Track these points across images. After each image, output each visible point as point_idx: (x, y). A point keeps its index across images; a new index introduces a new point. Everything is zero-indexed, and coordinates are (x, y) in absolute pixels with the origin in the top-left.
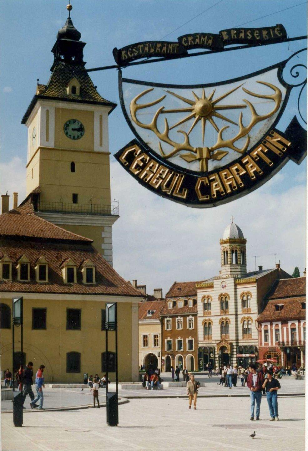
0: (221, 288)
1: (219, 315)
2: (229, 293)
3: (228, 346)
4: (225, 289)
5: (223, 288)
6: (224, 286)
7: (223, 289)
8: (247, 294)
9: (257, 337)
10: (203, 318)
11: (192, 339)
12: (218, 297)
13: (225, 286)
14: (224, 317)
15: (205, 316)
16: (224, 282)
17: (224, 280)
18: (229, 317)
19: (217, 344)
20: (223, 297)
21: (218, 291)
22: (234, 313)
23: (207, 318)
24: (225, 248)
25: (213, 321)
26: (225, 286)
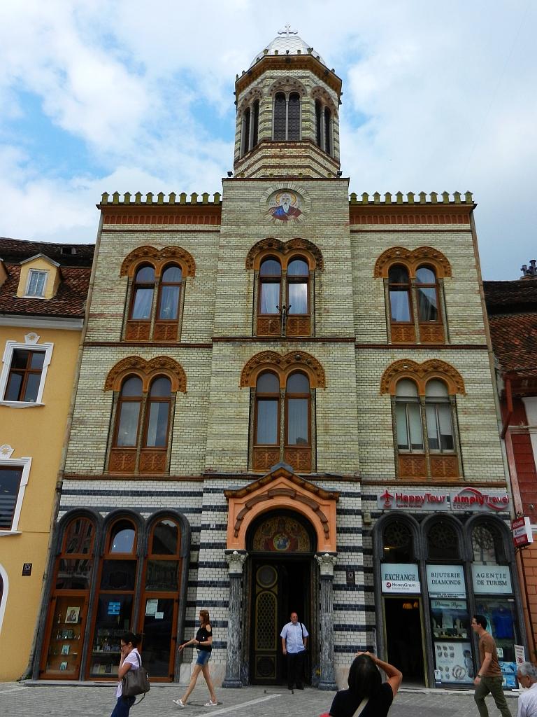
0: (270, 217)
1: (243, 340)
5: (284, 217)
6: (286, 209)
7: (278, 221)
10: (112, 357)
11: (15, 461)
12: (243, 254)
13: (291, 209)
15: (134, 345)
16: (289, 196)
17: (291, 185)
18: (314, 350)
19: (232, 495)
21: (253, 229)
23: (148, 355)
25: (189, 372)
26: (291, 209)
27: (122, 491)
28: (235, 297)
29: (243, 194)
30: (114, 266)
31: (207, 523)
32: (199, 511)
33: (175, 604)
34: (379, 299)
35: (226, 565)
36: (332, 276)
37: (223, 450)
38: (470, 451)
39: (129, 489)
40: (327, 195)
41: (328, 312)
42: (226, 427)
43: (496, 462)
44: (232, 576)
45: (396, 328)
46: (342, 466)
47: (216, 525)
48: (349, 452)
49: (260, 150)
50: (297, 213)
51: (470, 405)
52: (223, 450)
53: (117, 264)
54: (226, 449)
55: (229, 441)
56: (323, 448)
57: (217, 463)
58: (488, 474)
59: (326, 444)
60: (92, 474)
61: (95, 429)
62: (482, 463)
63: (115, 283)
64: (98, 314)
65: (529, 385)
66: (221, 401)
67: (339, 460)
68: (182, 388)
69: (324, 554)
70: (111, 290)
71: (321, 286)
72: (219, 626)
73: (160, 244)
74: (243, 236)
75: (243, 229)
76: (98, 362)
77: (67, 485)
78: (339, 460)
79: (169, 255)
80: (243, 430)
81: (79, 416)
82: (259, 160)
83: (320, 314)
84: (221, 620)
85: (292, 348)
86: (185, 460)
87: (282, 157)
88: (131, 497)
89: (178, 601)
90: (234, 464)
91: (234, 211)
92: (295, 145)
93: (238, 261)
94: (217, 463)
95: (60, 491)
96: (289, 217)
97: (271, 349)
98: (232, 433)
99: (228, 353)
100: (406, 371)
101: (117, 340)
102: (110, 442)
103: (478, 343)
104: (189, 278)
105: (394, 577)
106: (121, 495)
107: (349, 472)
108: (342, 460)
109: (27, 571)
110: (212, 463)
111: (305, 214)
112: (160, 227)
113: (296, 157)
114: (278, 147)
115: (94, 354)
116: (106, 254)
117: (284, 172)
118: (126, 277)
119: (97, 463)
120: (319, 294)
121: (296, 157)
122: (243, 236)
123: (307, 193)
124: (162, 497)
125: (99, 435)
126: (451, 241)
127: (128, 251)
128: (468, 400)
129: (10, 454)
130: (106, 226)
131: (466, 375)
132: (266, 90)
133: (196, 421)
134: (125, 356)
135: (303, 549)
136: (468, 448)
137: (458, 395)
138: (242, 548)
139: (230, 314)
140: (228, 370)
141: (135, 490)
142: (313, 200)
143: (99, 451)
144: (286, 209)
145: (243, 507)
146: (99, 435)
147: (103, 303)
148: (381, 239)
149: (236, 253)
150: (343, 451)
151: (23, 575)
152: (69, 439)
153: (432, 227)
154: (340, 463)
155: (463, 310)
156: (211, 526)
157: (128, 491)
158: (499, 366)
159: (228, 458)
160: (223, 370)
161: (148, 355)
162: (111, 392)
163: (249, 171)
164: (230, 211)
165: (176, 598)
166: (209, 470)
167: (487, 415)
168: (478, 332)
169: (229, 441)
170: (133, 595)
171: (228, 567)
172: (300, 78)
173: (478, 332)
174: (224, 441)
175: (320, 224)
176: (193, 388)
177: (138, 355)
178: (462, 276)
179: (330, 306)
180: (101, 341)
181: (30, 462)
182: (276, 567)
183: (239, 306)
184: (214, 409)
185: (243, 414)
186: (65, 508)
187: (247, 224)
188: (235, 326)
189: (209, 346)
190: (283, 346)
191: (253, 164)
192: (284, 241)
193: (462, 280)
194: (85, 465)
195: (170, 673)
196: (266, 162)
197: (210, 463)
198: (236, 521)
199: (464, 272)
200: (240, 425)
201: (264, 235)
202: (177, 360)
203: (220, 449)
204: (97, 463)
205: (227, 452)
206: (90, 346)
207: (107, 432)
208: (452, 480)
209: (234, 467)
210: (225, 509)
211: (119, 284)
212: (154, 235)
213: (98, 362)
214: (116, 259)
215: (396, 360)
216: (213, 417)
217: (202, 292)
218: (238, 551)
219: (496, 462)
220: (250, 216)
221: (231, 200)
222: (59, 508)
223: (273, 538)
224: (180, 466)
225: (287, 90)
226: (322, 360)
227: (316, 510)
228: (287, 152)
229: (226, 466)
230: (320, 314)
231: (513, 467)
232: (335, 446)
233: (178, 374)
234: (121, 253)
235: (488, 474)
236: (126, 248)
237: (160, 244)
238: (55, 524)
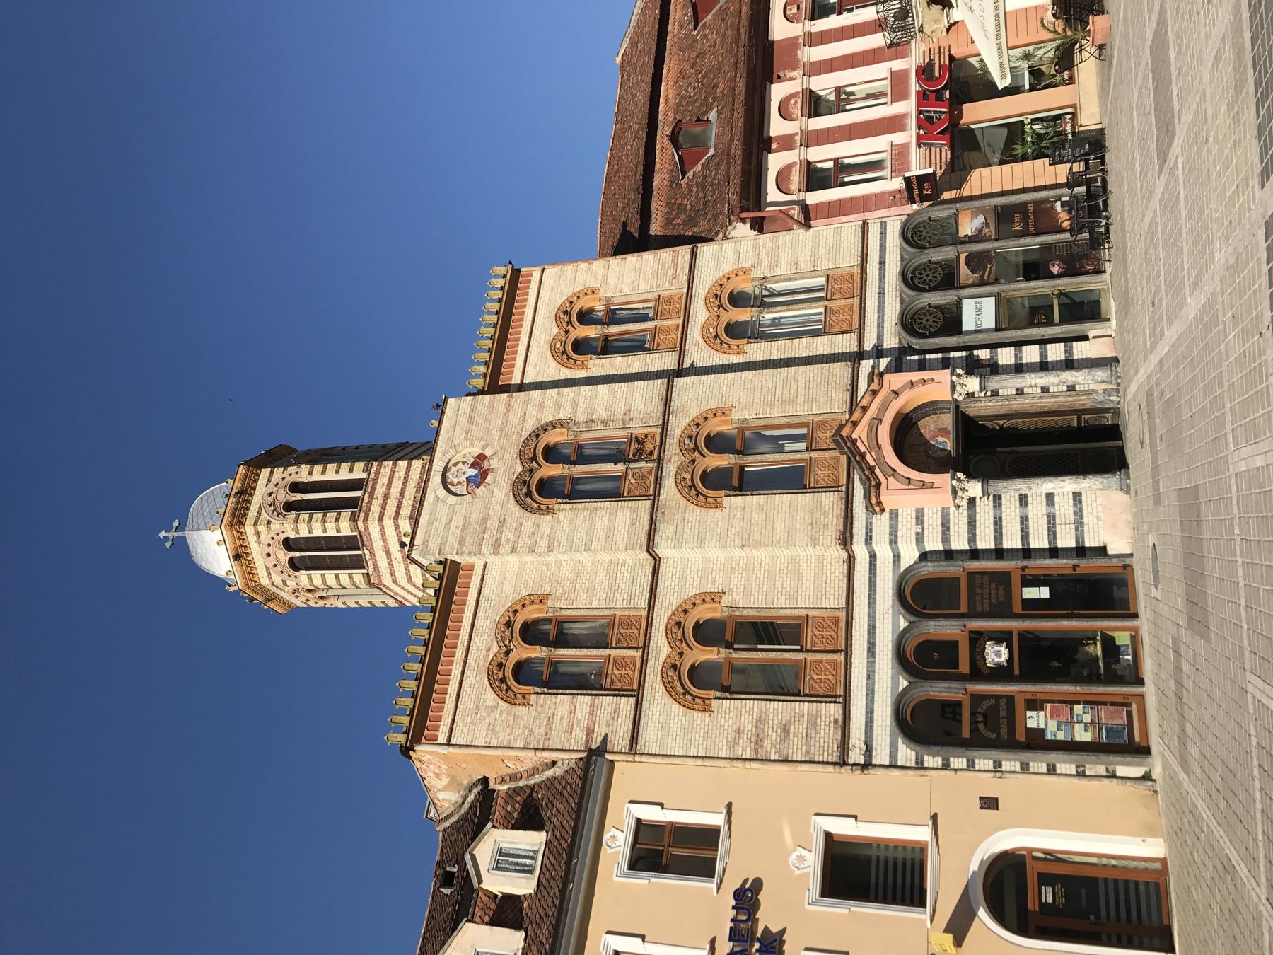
2: (529, 427)
3: (896, 393)
4: (493, 463)
5: (484, 474)
6: (474, 472)
7: (489, 480)
8: (569, 322)
9: (848, 227)
11: (818, 845)
12: (530, 519)
14: (673, 461)
20: (537, 477)
21: (495, 514)
22: (660, 384)
23: (661, 648)
24: (270, 500)
25: (692, 590)
26: (473, 466)
27: (868, 671)
28: (591, 526)
29: (437, 528)
30: (511, 718)
31: (914, 536)
32: (897, 557)
33: (1027, 572)
34: (617, 363)
35: (972, 501)
36: (580, 410)
37: (812, 524)
38: (823, 260)
39: (865, 661)
40: (463, 422)
41: (630, 411)
42: (779, 523)
43: (837, 233)
44: (985, 493)
45: (662, 314)
46: (838, 382)
47: (917, 524)
48: (820, 374)
49: (366, 529)
50: (482, 457)
51: (766, 262)
52: (812, 524)
53: (509, 714)
54: (810, 521)
55: (798, 518)
56: (814, 405)
57: (830, 530)
58: (853, 242)
59: (809, 401)
60: (840, 720)
61: (771, 722)
62: (838, 247)
63: (540, 714)
64: (588, 735)
65: (748, 200)
66: (740, 531)
67: (830, 386)
68: (714, 598)
69: (952, 382)
70: (551, 718)
71: (592, 421)
72: (1053, 511)
73: (489, 650)
74: (502, 523)
75: (493, 524)
76: (664, 728)
77: (856, 756)
78: (830, 386)
79: (508, 633)
80: (784, 502)
81: (748, 749)
82: (382, 528)
83: (631, 420)
84: (1044, 509)
85: (672, 449)
86: (824, 585)
87: (386, 496)
88: (877, 656)
89: (1023, 568)
90: (831, 509)
91: (461, 537)
92: (374, 480)
93: (538, 526)
94: (830, 530)
95: (867, 766)
96: (486, 468)
97: (672, 474)
98: (787, 516)
99: (672, 528)
100: (716, 329)
101: (632, 700)
102: (793, 698)
103: (687, 257)
104: (550, 603)
105: (979, 322)
106: (874, 672)
107: (846, 374)
108: (830, 382)
109: (990, 803)
110: (829, 537)
111: (483, 448)
112: (460, 653)
113: (391, 478)
114: (370, 503)
115: (650, 737)
116: (490, 732)
117: (411, 491)
118: (533, 697)
119: (823, 713)
120: (602, 422)
121: (391, 478)
122: (502, 523)
123: (455, 447)
124: (877, 612)
125: (780, 714)
126: (553, 289)
127: (490, 696)
128: (760, 264)
129: (804, 852)
130: (442, 738)
131: (728, 267)
132: (275, 526)
133: (766, 575)
134: (660, 688)
135: (947, 420)
136: (819, 262)
137: (753, 274)
138: (948, 476)
139: (616, 530)
140: (697, 526)
141: (865, 653)
142: (466, 438)
143: (806, 712)
144: (474, 472)
145: (891, 479)
146: (780, 714)
147: (570, 729)
148: (536, 365)
149: (526, 530)
150: (819, 381)
151: (997, 809)
152: (786, 761)
153: (529, 311)
154: (834, 384)
155: (645, 273)
156: (919, 530)
157: (868, 662)
158: (721, 235)
159: (822, 517)
160: (696, 532)
161: (661, 648)
162: (715, 703)
163: (392, 550)
164: (460, 543)
165: (1020, 572)
166: (839, 539)
167: (781, 245)
168: (675, 260)
169: (798, 518)
170: (1020, 634)
171: (974, 499)
172: (269, 481)
173: (675, 260)
174: (798, 524)
175: (504, 425)
176: (717, 584)
177: (660, 667)
178: (600, 277)
179: (621, 408)
180: (631, 726)
181: (820, 819)
182: (971, 457)
183: (606, 519)
184: (751, 541)
185: (761, 503)
186: (893, 754)
187: (485, 520)
188: (633, 523)
189: (657, 561)
190: (670, 460)
191: (384, 541)
192: (519, 468)
193: (606, 276)
194: (827, 731)
195: (1121, 571)
196: (390, 516)
197: (829, 540)
198: (911, 487)
199: (596, 274)
200: (776, 506)
201: (507, 495)
202: (674, 608)
203: (810, 528)
204: (823, 713)
205: (814, 519)
206: (637, 743)
207: (776, 702)
208: (857, 278)
209: (835, 508)
210: (894, 515)
211: (542, 706)
212: (471, 661)
213: (664, 728)
214: (501, 716)
215: (701, 340)
216: (763, 540)
217: (574, 582)
218: (952, 480)
219: (837, 233)
220: (474, 516)
221: (443, 543)
222: (893, 766)
223: (934, 458)
224: (832, 592)
225: (283, 496)
226: (694, 413)
227: (896, 393)
228: (380, 489)
229: (835, 519)
230: (631, 420)
231: (844, 219)
232: (811, 391)
233: (694, 604)
234: (492, 709)
235: (853, 242)
236: (485, 701)
237: (489, 650)
238: (920, 766)
